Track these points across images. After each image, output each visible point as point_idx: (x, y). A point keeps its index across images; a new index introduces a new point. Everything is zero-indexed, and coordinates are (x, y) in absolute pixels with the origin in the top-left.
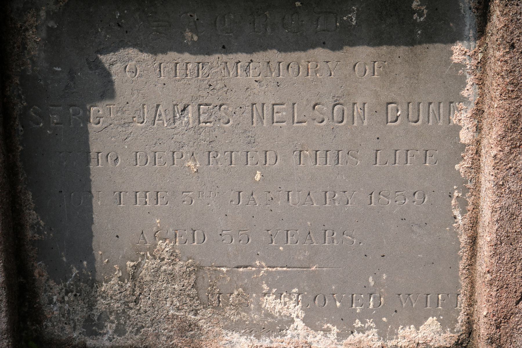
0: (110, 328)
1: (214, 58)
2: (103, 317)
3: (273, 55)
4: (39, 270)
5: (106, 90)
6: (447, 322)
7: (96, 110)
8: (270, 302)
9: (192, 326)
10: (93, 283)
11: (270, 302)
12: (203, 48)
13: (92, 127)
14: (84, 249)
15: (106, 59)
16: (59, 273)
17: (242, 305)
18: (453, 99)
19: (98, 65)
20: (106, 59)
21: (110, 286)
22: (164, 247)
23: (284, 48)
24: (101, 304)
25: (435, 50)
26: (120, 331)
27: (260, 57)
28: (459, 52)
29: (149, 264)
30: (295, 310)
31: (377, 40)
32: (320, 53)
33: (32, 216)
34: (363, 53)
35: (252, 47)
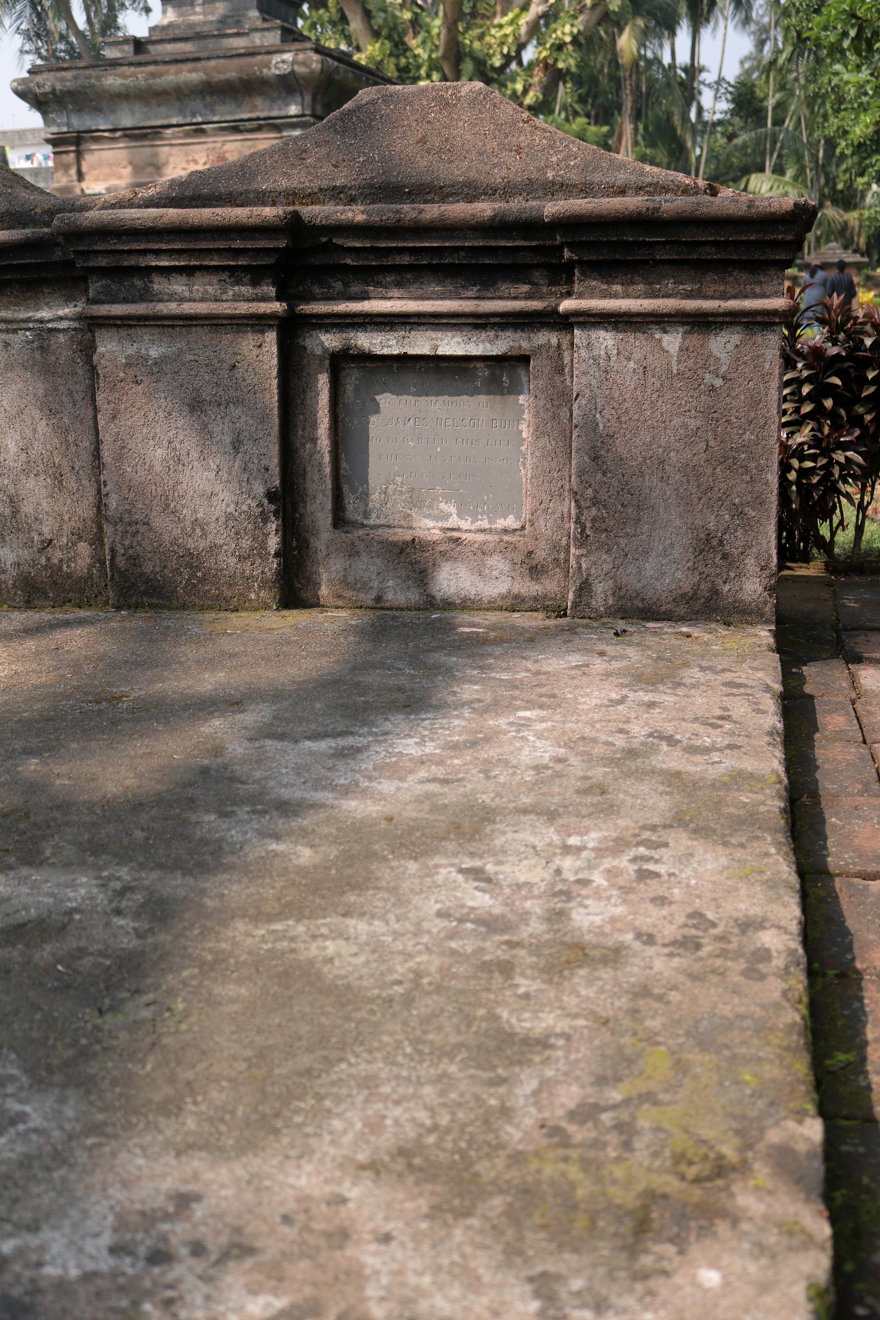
0: (374, 516)
1: (423, 398)
2: (371, 511)
3: (446, 398)
4: (345, 488)
5: (377, 410)
6: (518, 517)
7: (373, 419)
8: (442, 506)
9: (409, 515)
10: (367, 495)
11: (442, 506)
12: (418, 394)
13: (371, 426)
14: (364, 479)
15: (377, 397)
16: (354, 490)
17: (430, 507)
18: (520, 419)
19: (374, 400)
20: (377, 397)
21: (375, 497)
22: (399, 479)
23: (451, 395)
24: (371, 505)
25: (512, 397)
26: (378, 517)
27: (441, 398)
28: (522, 399)
29: (392, 487)
30: (453, 510)
31: (488, 393)
32: (465, 397)
33: (344, 464)
34: (483, 398)
35: (437, 394)
